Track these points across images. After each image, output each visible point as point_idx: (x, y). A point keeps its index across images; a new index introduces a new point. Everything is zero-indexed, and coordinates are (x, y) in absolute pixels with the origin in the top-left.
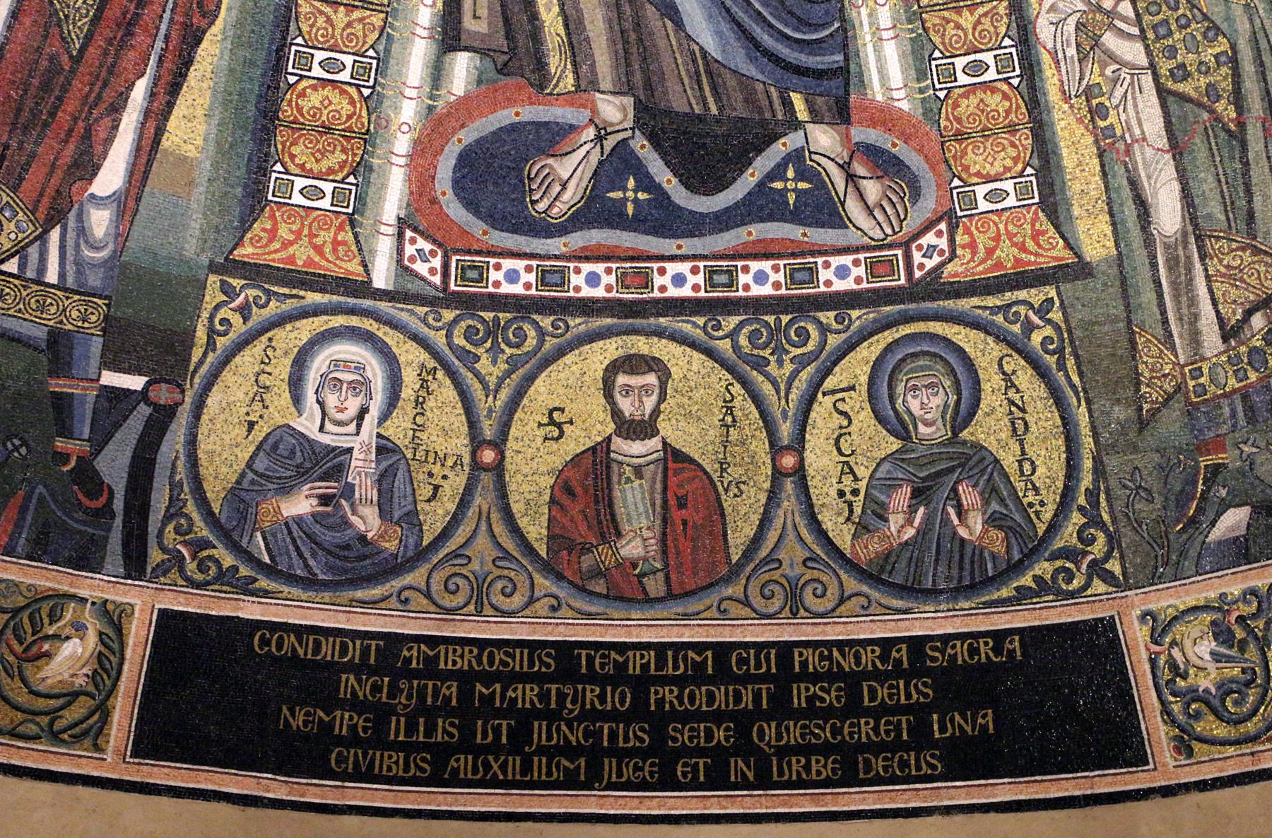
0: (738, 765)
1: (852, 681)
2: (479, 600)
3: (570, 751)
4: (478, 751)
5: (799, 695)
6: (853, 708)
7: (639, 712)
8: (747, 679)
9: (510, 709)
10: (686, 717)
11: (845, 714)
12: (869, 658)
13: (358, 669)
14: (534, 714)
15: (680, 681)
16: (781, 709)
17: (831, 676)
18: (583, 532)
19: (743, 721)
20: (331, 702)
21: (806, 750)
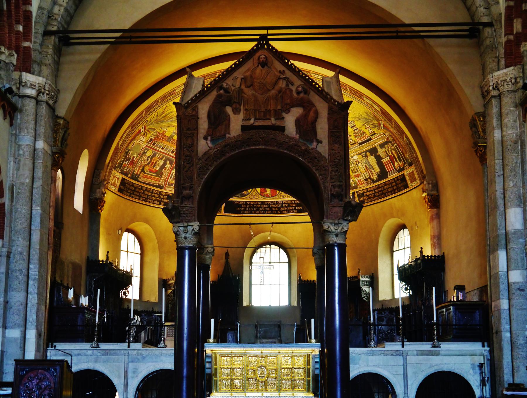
0: (278, 212)
1: (289, 204)
2: (254, 198)
3: (263, 211)
4: (255, 211)
5: (284, 205)
6: (289, 206)
7: (269, 207)
8: (279, 204)
9: (257, 207)
10: (274, 207)
11: (288, 207)
12: (290, 202)
13: (243, 204)
14: (259, 207)
15: (273, 204)
16: (282, 207)
17: (287, 204)
18: (263, 191)
19: (279, 208)
20: (241, 207)
21: (285, 210)
